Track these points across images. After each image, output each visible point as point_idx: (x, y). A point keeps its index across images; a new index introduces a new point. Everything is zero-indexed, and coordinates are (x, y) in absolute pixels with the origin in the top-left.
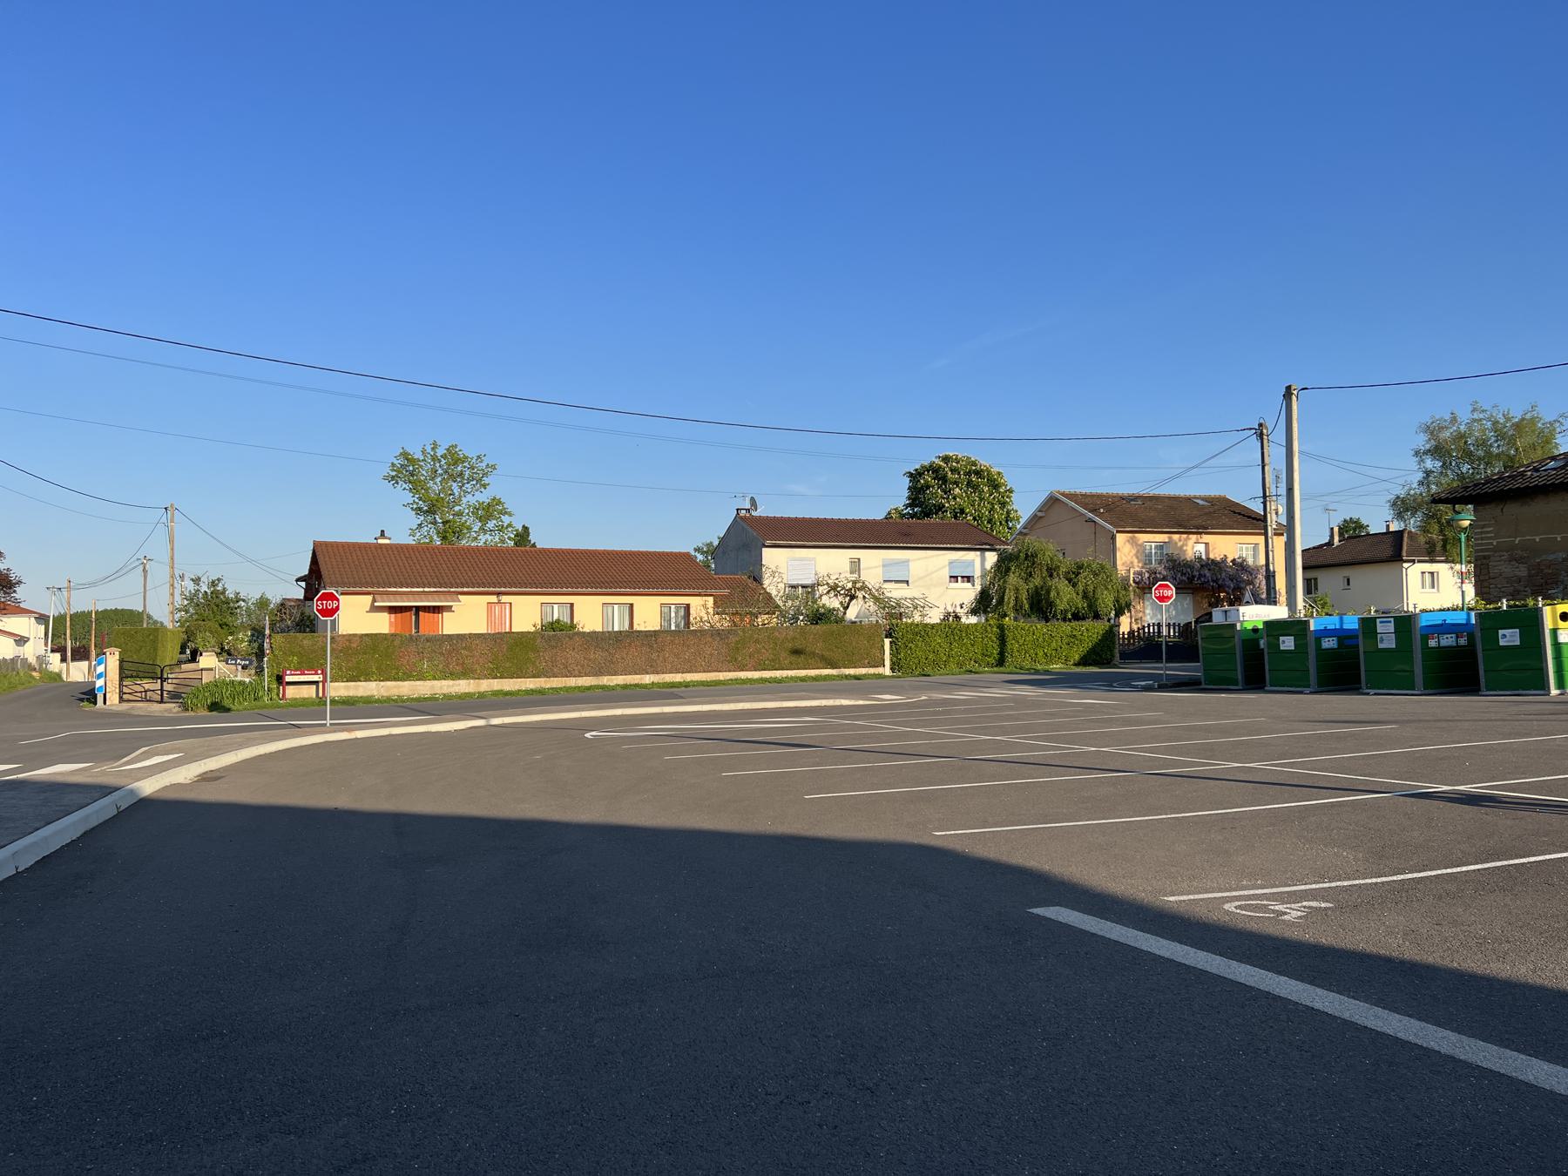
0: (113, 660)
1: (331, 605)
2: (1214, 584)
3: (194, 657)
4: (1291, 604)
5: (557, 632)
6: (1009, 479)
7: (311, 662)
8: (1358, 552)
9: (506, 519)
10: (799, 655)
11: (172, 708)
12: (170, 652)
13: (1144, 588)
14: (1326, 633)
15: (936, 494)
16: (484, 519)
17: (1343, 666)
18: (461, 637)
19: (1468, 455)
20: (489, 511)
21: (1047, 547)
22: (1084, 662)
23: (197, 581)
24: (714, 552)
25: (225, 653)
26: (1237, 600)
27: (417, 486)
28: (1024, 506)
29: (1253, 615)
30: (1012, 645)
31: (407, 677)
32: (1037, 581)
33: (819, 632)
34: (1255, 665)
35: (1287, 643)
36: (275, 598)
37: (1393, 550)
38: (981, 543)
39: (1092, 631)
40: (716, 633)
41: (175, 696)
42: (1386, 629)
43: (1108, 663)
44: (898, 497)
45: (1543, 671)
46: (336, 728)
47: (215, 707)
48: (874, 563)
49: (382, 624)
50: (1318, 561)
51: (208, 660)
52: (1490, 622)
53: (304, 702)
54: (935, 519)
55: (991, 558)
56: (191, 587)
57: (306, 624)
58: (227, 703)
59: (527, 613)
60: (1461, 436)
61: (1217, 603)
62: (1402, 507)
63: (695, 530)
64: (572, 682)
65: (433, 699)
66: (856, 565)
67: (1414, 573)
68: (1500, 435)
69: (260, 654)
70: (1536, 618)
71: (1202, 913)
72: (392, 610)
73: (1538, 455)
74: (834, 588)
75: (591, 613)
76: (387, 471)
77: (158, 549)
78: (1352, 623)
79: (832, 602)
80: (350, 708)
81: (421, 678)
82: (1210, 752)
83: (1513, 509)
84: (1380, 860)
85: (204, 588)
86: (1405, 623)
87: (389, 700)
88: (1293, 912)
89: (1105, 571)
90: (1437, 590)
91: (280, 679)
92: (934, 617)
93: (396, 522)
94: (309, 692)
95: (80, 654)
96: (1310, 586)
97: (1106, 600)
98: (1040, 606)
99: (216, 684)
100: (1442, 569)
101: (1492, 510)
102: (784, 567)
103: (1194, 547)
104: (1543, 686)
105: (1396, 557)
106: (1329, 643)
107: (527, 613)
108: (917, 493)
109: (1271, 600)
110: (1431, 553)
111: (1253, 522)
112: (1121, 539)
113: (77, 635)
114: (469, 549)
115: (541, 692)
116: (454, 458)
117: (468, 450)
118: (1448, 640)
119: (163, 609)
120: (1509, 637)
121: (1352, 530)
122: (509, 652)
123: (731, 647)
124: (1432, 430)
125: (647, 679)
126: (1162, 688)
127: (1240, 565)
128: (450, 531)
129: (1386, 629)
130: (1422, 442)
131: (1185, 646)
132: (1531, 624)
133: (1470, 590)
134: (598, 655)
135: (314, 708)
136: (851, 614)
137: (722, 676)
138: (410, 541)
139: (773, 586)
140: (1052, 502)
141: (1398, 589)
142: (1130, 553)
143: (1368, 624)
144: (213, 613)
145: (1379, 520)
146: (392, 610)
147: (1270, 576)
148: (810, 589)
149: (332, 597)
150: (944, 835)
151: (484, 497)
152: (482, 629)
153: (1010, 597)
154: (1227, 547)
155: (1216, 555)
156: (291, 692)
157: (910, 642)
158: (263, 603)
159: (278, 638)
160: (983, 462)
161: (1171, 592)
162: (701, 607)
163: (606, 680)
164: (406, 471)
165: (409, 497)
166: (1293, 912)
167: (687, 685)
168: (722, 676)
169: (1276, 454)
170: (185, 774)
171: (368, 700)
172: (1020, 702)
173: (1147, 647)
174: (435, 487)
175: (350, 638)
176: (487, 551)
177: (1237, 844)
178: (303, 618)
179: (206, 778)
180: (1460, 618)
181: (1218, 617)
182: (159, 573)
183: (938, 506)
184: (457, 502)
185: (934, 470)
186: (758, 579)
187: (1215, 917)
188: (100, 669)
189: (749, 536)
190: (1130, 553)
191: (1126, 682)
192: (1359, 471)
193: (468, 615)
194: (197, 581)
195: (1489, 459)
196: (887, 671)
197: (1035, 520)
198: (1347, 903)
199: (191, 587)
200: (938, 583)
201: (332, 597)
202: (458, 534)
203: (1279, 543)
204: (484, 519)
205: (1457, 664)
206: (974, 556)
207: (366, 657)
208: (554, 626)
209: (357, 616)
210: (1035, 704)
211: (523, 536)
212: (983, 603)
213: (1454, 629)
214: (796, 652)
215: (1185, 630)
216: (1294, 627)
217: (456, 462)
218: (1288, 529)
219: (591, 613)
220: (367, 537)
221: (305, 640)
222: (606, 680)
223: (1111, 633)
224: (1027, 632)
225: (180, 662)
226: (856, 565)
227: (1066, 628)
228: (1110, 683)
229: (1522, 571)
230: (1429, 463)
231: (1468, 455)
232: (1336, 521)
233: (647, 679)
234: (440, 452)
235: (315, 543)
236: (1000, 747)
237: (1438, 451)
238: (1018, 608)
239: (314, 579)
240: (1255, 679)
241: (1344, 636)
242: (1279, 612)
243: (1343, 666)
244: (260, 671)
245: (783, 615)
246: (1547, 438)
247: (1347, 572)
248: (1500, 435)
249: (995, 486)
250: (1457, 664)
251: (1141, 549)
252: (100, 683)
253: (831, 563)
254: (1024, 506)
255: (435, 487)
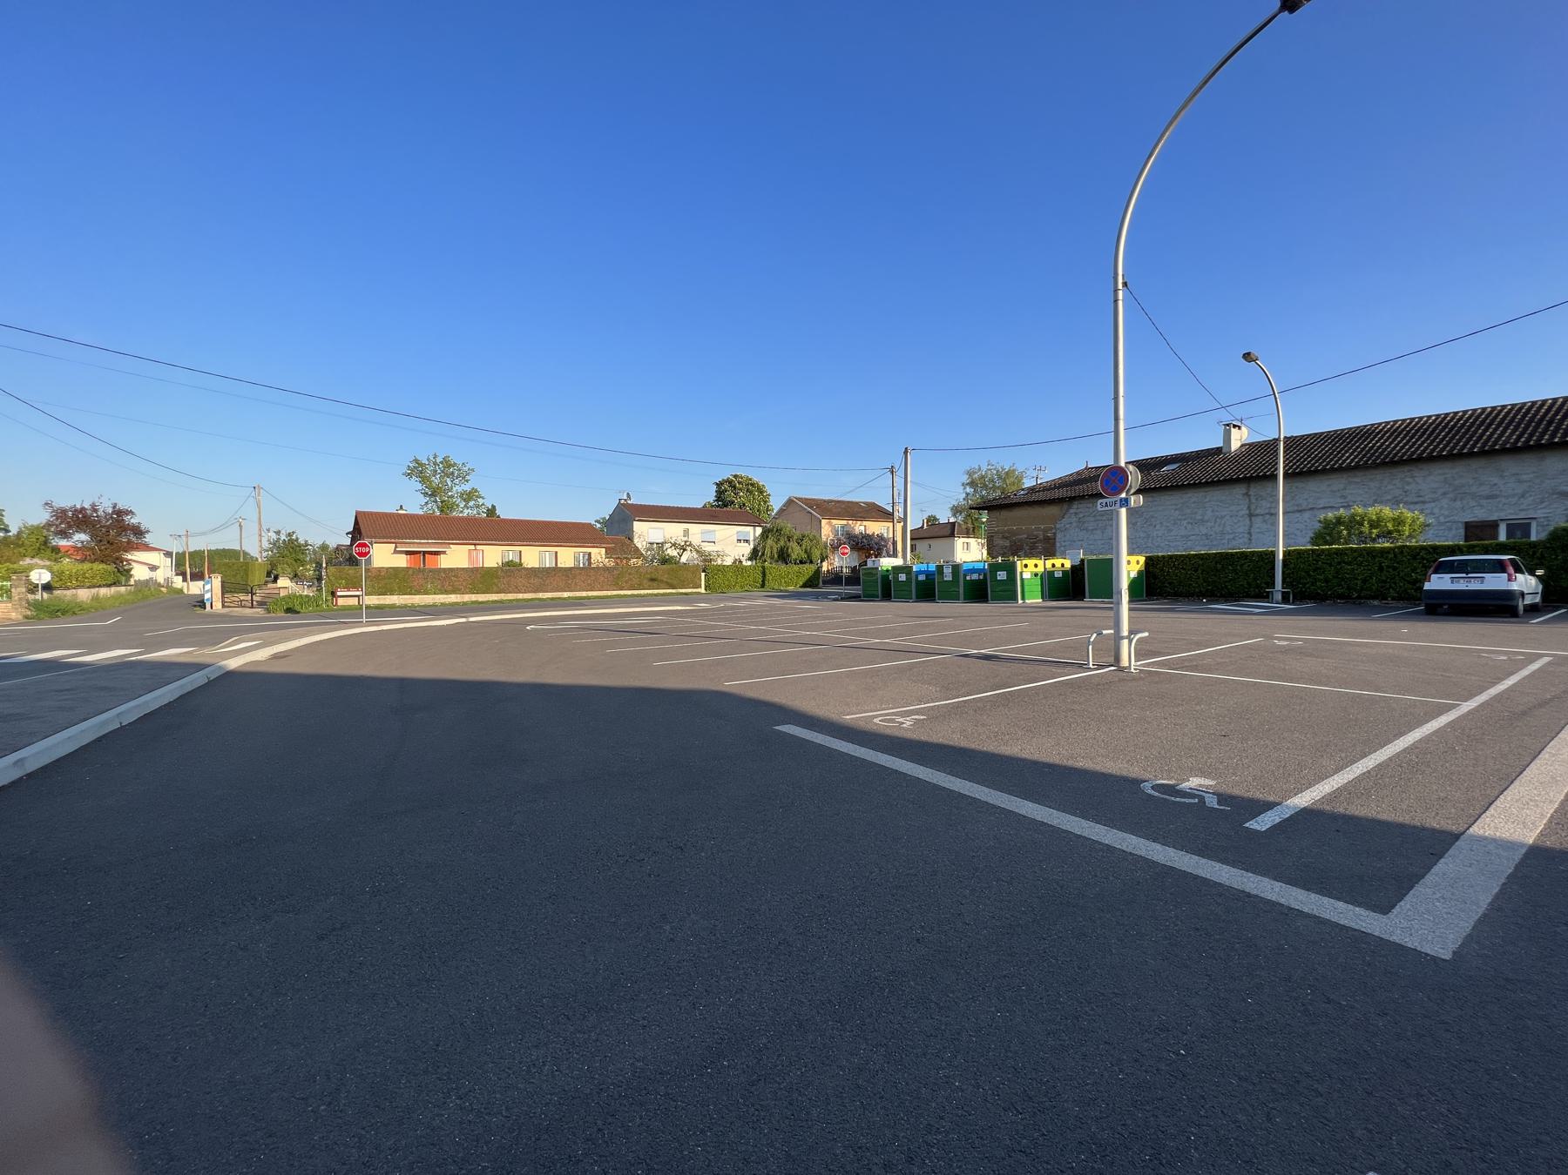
0: (217, 581)
1: (364, 550)
2: (868, 547)
3: (275, 580)
4: (904, 557)
5: (512, 569)
6: (768, 489)
7: (353, 584)
8: (935, 533)
9: (481, 501)
10: (654, 581)
11: (260, 611)
12: (258, 576)
13: (835, 548)
14: (920, 572)
15: (730, 495)
16: (467, 501)
17: (928, 589)
18: (451, 570)
19: (985, 486)
20: (469, 496)
21: (788, 526)
22: (804, 586)
23: (278, 533)
24: (606, 523)
25: (295, 577)
26: (878, 555)
27: (424, 479)
28: (776, 504)
29: (886, 563)
30: (769, 577)
31: (418, 593)
32: (782, 543)
33: (666, 570)
34: (887, 588)
35: (902, 577)
36: (332, 544)
37: (950, 531)
38: (752, 521)
39: (808, 570)
40: (606, 569)
41: (261, 604)
42: (948, 571)
43: (816, 586)
44: (710, 496)
45: (1015, 592)
46: (369, 624)
47: (289, 610)
48: (697, 532)
49: (401, 561)
50: (918, 536)
51: (283, 582)
52: (994, 568)
53: (350, 608)
54: (729, 508)
55: (759, 530)
56: (274, 537)
57: (352, 561)
58: (298, 608)
59: (493, 556)
60: (983, 477)
61: (869, 556)
62: (956, 510)
63: (594, 511)
64: (520, 596)
65: (434, 605)
66: (686, 532)
67: (959, 542)
68: (1000, 477)
69: (319, 579)
70: (1013, 565)
71: (862, 725)
72: (407, 553)
73: (1014, 488)
74: (674, 545)
75: (533, 556)
76: (405, 470)
77: (250, 512)
78: (932, 567)
79: (673, 552)
80: (380, 611)
81: (426, 593)
82: (866, 634)
83: (1005, 514)
84: (947, 691)
85: (283, 537)
86: (956, 568)
87: (406, 606)
88: (908, 723)
89: (816, 539)
90: (970, 552)
91: (333, 594)
92: (728, 561)
93: (413, 502)
94: (354, 602)
95: (197, 576)
96: (913, 548)
97: (816, 554)
98: (783, 557)
99: (289, 597)
100: (972, 541)
101: (996, 514)
102: (646, 533)
103: (859, 527)
104: (1015, 598)
105: (952, 535)
106: (922, 578)
107: (493, 556)
108: (720, 494)
109: (895, 555)
110: (968, 533)
111: (887, 515)
112: (824, 522)
113: (193, 565)
114: (454, 518)
115: (501, 602)
116: (447, 463)
117: (453, 459)
118: (975, 577)
119: (255, 547)
120: (1002, 575)
121: (932, 520)
122: (480, 579)
123: (612, 577)
124: (970, 474)
125: (566, 595)
126: (843, 599)
127: (881, 537)
128: (446, 507)
129: (948, 571)
130: (965, 479)
131: (854, 578)
132: (1011, 569)
133: (985, 552)
134: (536, 581)
135: (354, 612)
136: (684, 559)
137: (609, 593)
138: (421, 512)
139: (640, 543)
140: (790, 502)
141: (952, 550)
142: (828, 530)
143: (940, 568)
144: (289, 554)
145: (945, 517)
146: (407, 553)
147: (895, 543)
148: (661, 545)
149: (365, 545)
150: (731, 685)
151: (467, 487)
152: (465, 564)
153: (768, 551)
154: (875, 528)
155: (869, 532)
156: (341, 602)
157: (714, 574)
158: (324, 547)
159: (332, 569)
160: (755, 479)
161: (848, 550)
162: (598, 555)
163: (541, 595)
164: (417, 470)
165: (419, 486)
166: (908, 723)
167: (588, 598)
168: (609, 593)
169: (899, 482)
170: (262, 654)
171: (393, 606)
172: (773, 607)
173: (835, 579)
174: (436, 480)
175: (380, 570)
176: (468, 520)
177: (875, 685)
178: (349, 558)
179: (276, 657)
180: (980, 566)
181: (870, 564)
182: (251, 528)
183: (731, 502)
184: (450, 490)
185: (730, 482)
186: (631, 539)
187: (869, 727)
188: (208, 587)
189: (626, 515)
190: (828, 530)
191: (825, 596)
192: (936, 493)
193: (456, 557)
194: (278, 533)
195: (994, 488)
196: (702, 590)
197: (781, 511)
198: (935, 716)
199: (274, 537)
200: (731, 543)
201: (365, 545)
202: (452, 507)
203: (899, 526)
204: (467, 501)
205: (982, 588)
206: (750, 529)
207: (389, 581)
208: (509, 564)
209: (384, 556)
210: (781, 608)
211: (491, 511)
212: (754, 555)
213: (978, 571)
214: (652, 580)
215: (854, 569)
216: (906, 569)
217: (450, 466)
218: (905, 520)
219: (533, 556)
220: (390, 508)
221: (350, 570)
222: (541, 595)
223: (818, 571)
224: (776, 569)
225: (266, 583)
226: (686, 532)
227: (796, 568)
228: (817, 597)
229: (1007, 543)
230: (968, 490)
231: (985, 486)
232: (925, 516)
233: (566, 595)
234: (439, 460)
235: (358, 513)
236: (767, 632)
237: (972, 484)
238: (772, 557)
239: (356, 533)
240: (887, 595)
241: (928, 574)
242: (898, 562)
243: (928, 589)
244: (320, 590)
245: (645, 558)
246: (1019, 479)
247: (931, 542)
248: (1000, 477)
249: (761, 492)
250: (982, 588)
251: (833, 527)
252: (207, 596)
253: (672, 531)
254: (776, 504)
255: (436, 480)
